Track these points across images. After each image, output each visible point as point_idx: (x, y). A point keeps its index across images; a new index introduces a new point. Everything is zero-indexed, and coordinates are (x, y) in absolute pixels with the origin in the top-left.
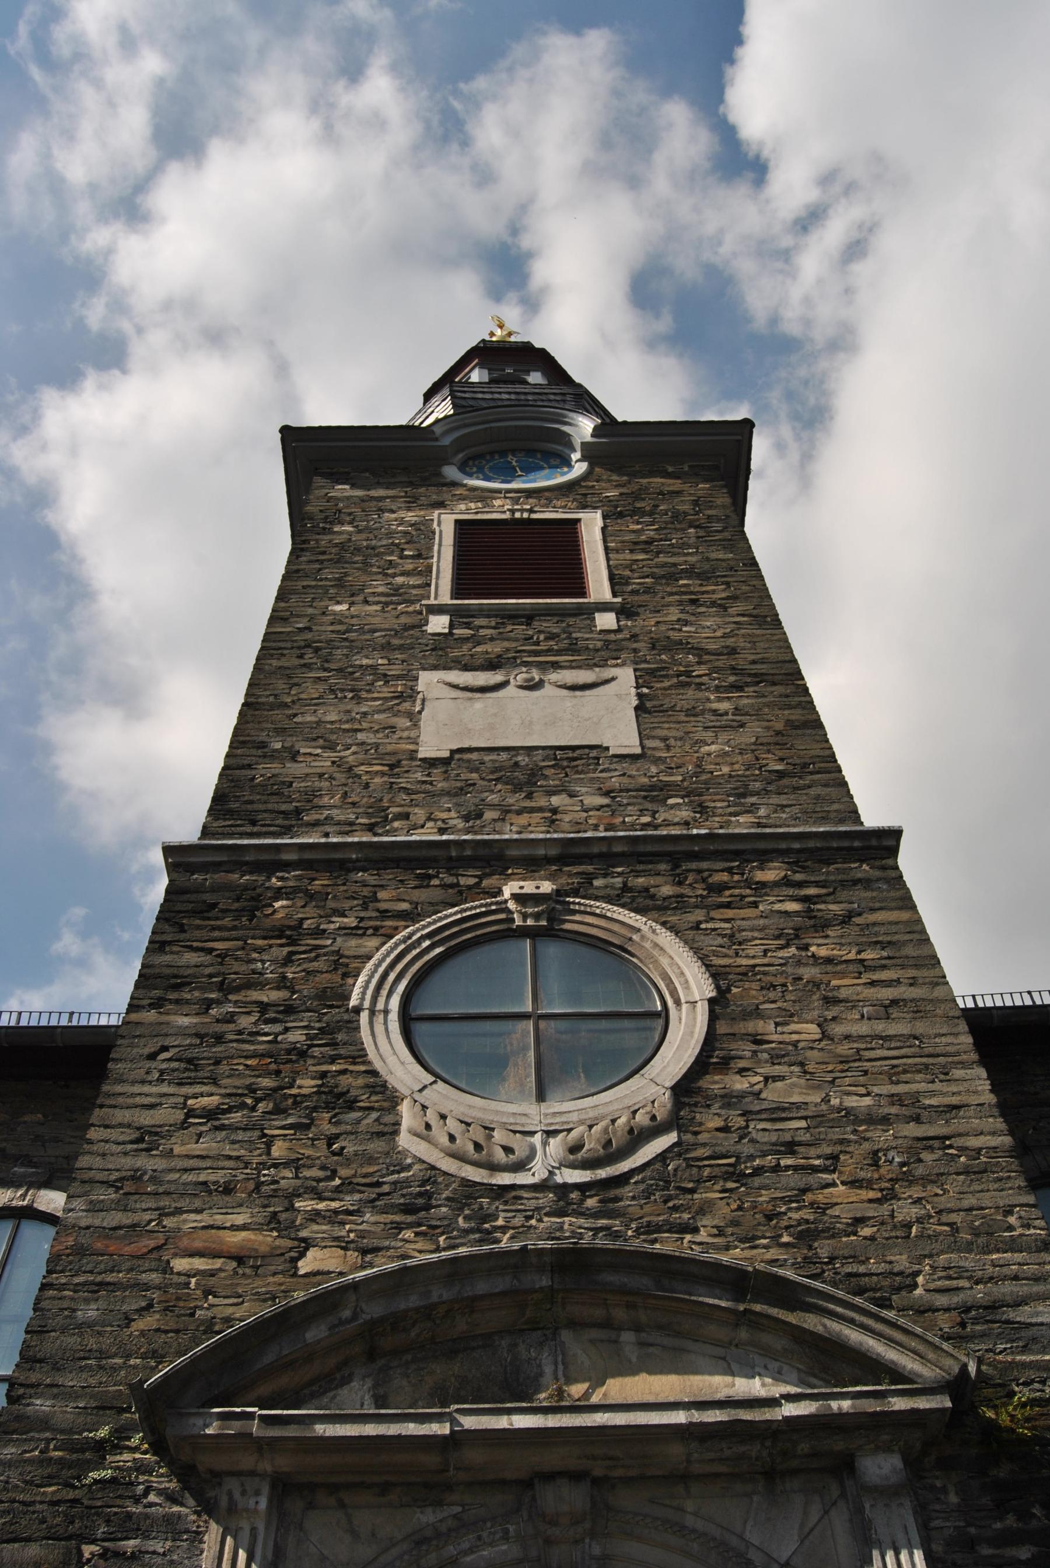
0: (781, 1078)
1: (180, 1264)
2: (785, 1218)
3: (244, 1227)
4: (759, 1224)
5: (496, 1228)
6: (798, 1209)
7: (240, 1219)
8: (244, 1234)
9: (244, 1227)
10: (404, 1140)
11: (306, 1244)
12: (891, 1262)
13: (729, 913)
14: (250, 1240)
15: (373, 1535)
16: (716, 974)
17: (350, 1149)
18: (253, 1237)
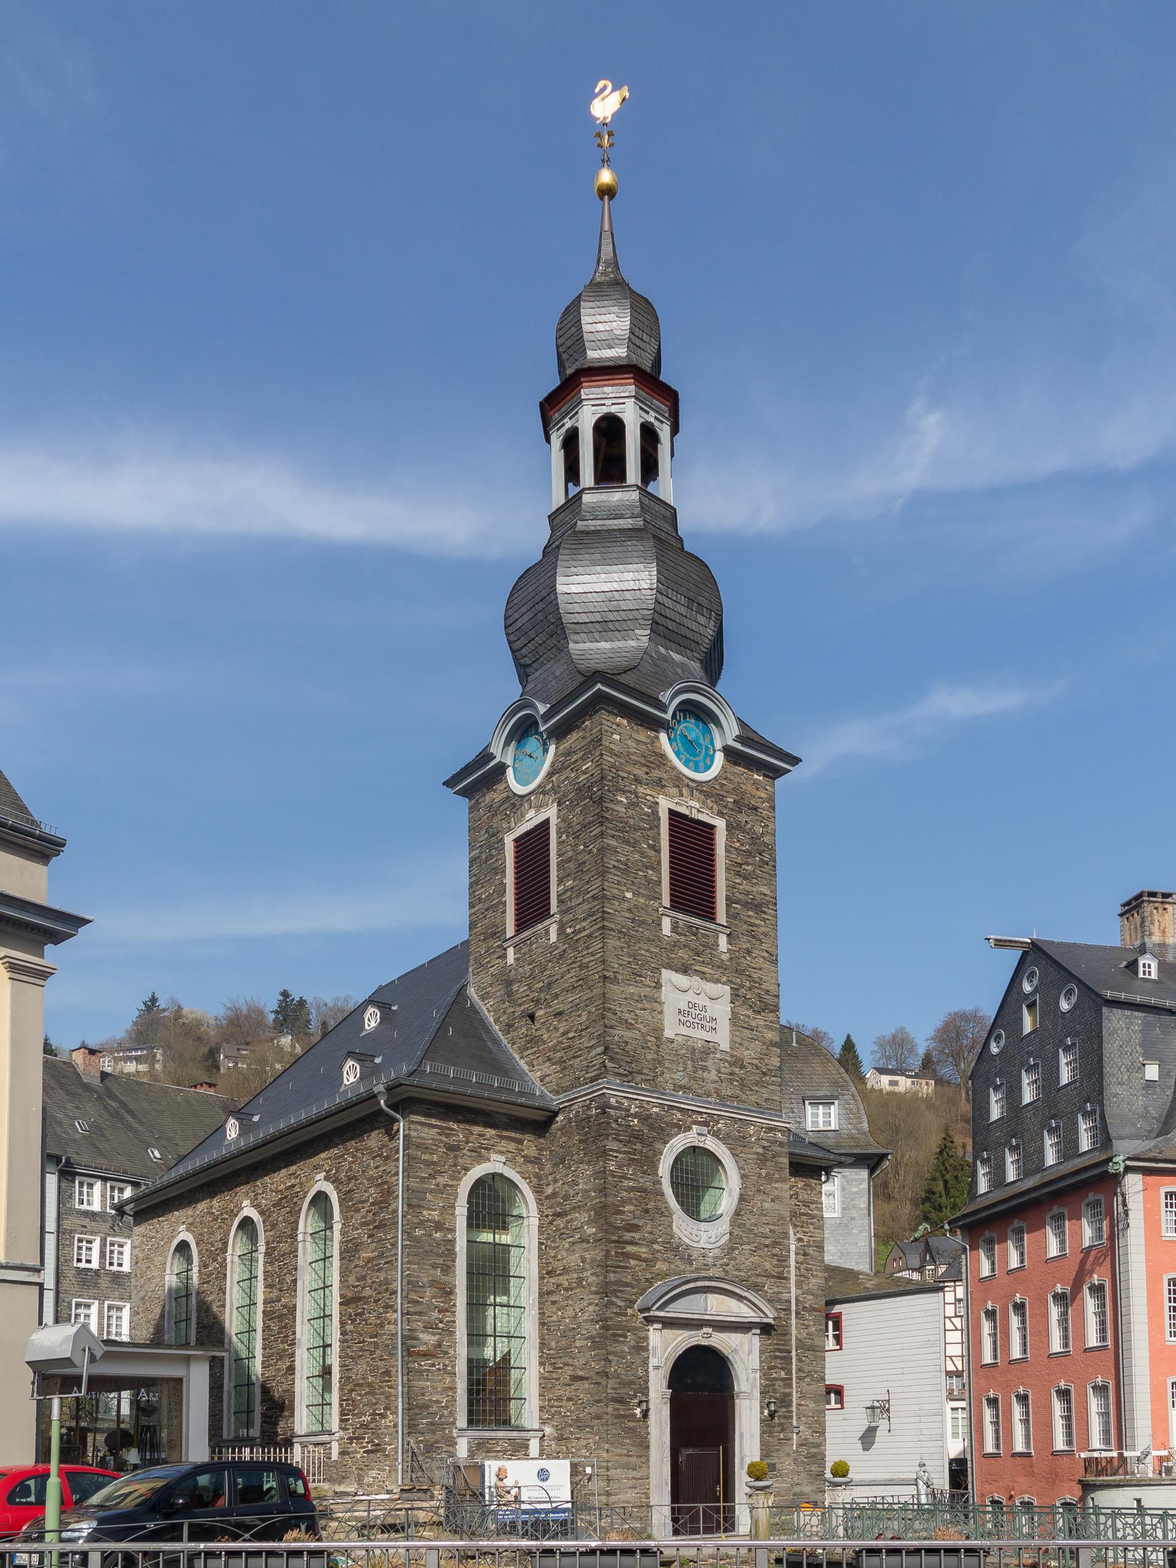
1: (633, 1262)
7: (644, 1250)
16: (743, 1177)
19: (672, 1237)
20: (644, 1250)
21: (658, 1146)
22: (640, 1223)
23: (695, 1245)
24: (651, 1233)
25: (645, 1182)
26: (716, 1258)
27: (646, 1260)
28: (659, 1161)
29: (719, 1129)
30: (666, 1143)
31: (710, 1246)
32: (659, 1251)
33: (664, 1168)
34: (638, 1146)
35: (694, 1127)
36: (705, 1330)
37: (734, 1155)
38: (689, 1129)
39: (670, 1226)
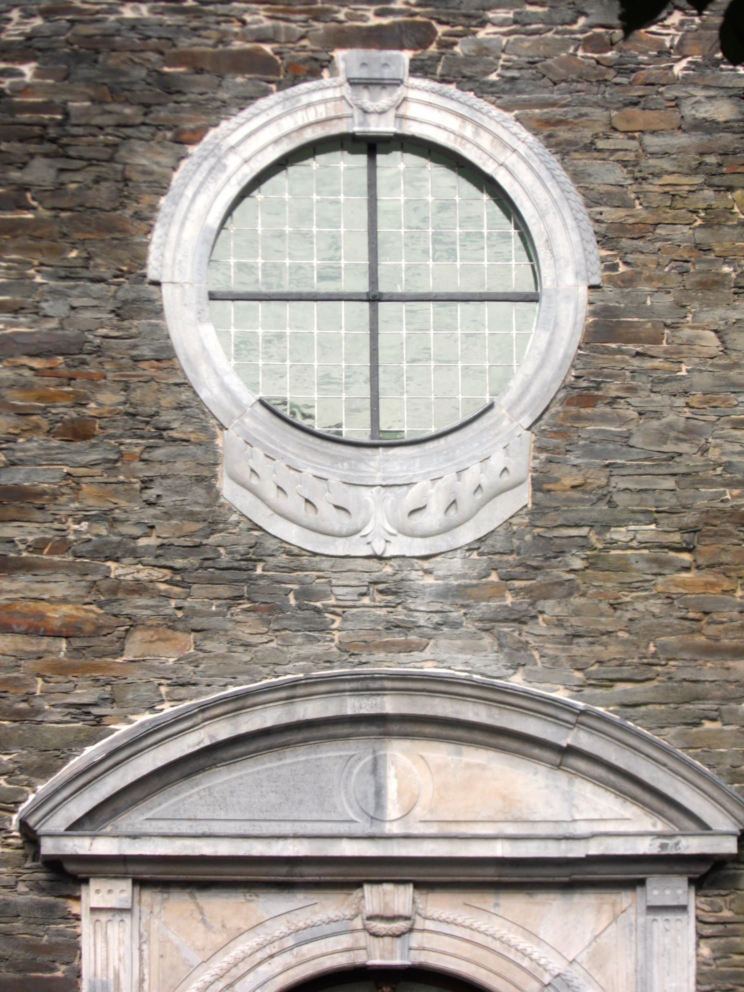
0: (657, 414)
2: (630, 608)
3: (64, 600)
4: (602, 615)
5: (326, 608)
6: (646, 598)
8: (66, 609)
9: (64, 600)
10: (227, 489)
11: (134, 624)
12: (728, 669)
13: (640, 117)
14: (72, 616)
15: (223, 926)
17: (168, 500)
18: (74, 612)
19: (213, 525)
20: (60, 587)
21: (142, 157)
22: (43, 479)
23: (339, 548)
24: (105, 517)
25: (86, 311)
26: (458, 594)
27: (69, 631)
28: (146, 219)
29: (483, 50)
30: (184, 139)
31: (419, 547)
32: (139, 588)
33: (179, 244)
34: (41, 172)
35: (339, 54)
36: (374, 898)
37: (562, 150)
38: (314, 68)
39: (206, 480)
